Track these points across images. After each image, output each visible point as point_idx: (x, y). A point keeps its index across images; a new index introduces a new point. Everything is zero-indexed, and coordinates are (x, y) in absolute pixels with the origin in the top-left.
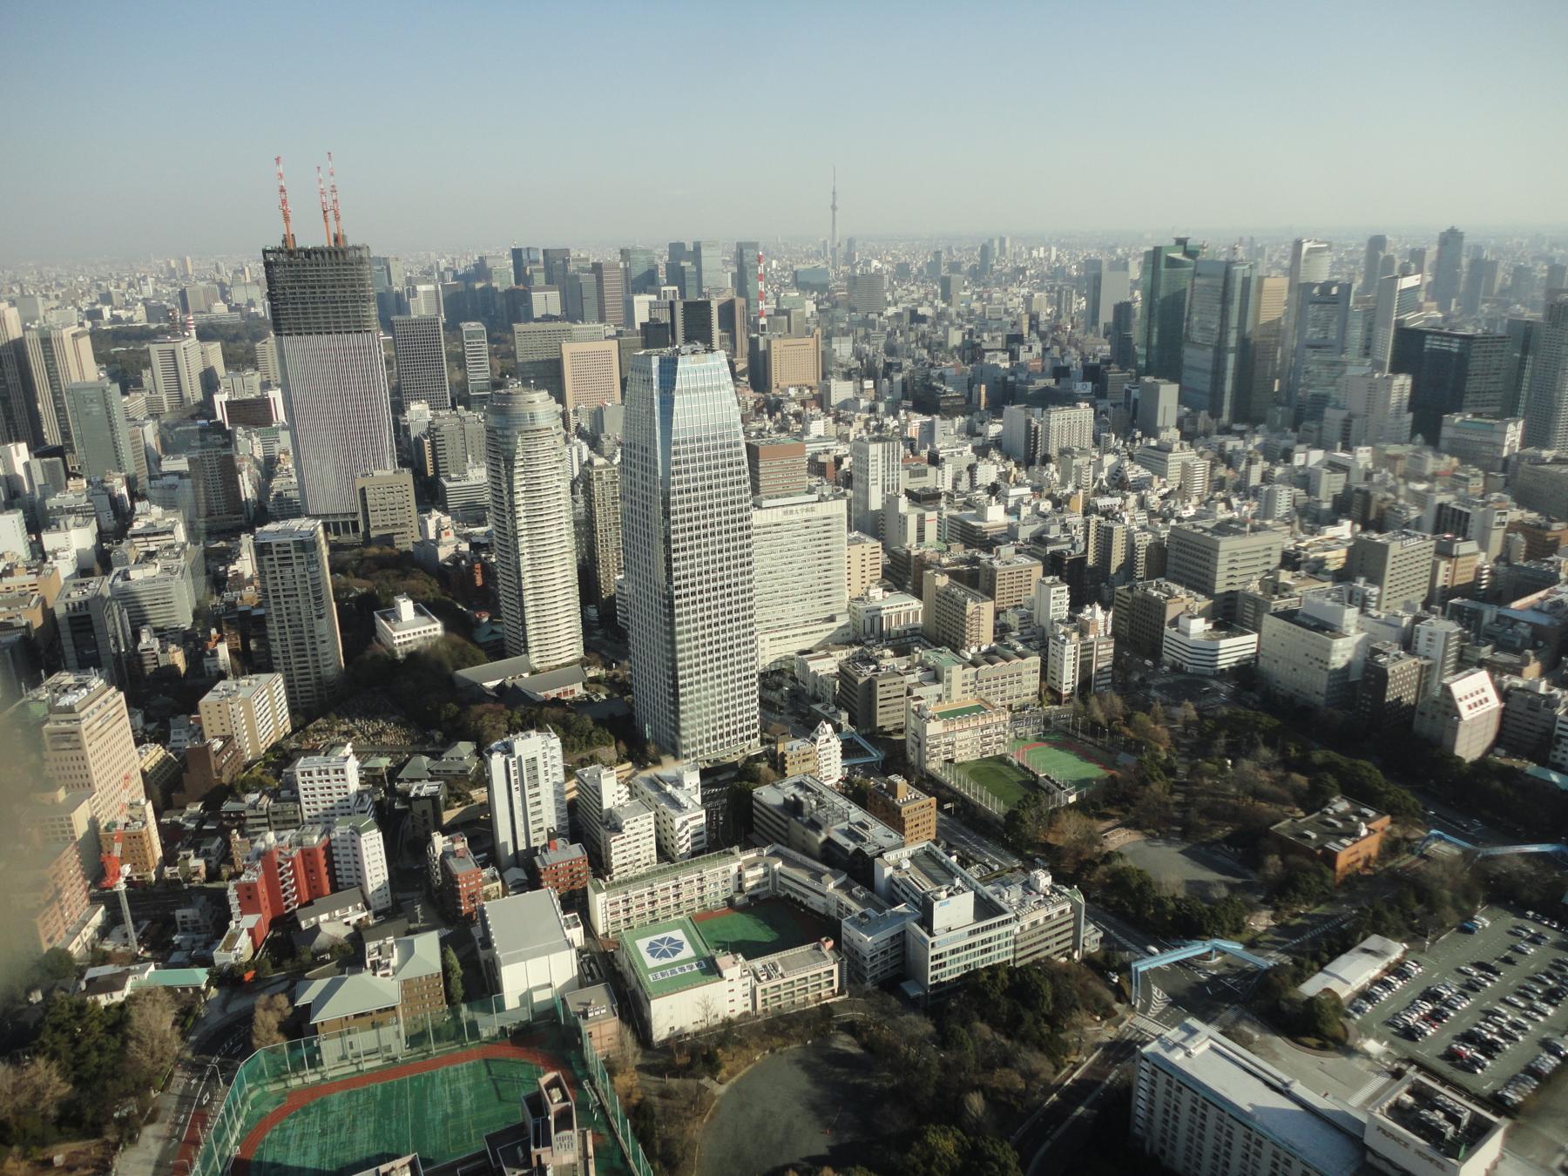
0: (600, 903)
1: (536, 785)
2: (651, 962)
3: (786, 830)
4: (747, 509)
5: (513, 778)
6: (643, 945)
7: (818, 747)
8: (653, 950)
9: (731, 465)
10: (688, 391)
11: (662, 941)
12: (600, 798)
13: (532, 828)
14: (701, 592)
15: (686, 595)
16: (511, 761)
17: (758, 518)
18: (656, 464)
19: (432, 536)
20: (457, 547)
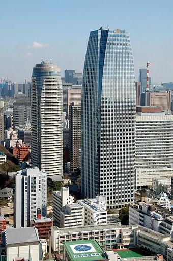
0: (56, 233)
1: (35, 191)
2: (75, 252)
3: (143, 221)
4: (134, 114)
5: (25, 185)
6: (73, 247)
7: (160, 202)
8: (76, 248)
9: (128, 106)
10: (112, 44)
11: (82, 246)
12: (61, 200)
13: (31, 210)
14: (112, 139)
15: (105, 139)
16: (25, 177)
17: (138, 118)
18: (97, 70)
19: (8, 137)
20: (17, 142)
